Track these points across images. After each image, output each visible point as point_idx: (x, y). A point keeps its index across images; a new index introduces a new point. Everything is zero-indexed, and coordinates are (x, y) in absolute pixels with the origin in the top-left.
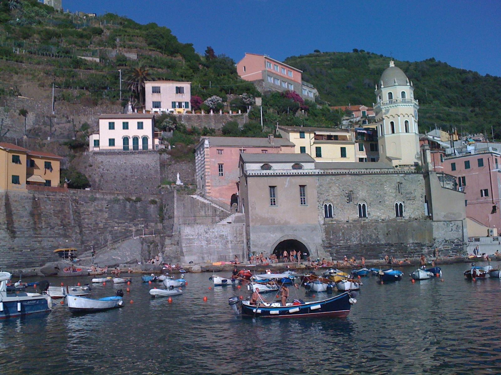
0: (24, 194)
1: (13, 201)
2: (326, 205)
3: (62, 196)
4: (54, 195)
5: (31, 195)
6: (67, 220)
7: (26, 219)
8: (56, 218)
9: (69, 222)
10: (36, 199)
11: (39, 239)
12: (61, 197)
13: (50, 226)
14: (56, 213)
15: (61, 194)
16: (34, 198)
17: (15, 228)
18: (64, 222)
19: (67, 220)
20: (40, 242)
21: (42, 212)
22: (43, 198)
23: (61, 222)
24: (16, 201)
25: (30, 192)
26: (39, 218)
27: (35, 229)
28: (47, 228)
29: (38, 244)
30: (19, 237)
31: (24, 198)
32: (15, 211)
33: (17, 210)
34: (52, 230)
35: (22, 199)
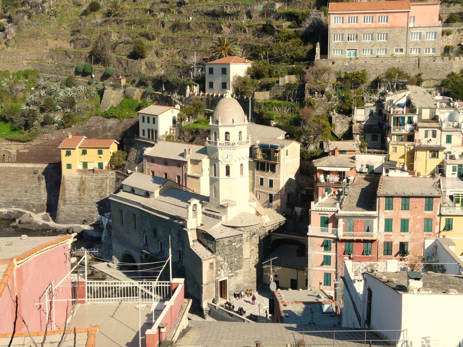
2: (146, 235)
3: (103, 176)
4: (96, 176)
5: (80, 176)
6: (104, 193)
7: (74, 192)
9: (105, 195)
11: (82, 206)
12: (101, 177)
14: (96, 188)
15: (102, 174)
16: (82, 178)
18: (102, 195)
19: (104, 193)
20: (82, 208)
21: (86, 188)
22: (88, 178)
23: (99, 194)
24: (69, 180)
27: (80, 199)
28: (88, 198)
29: (81, 209)
30: (68, 204)
32: (67, 188)
33: (69, 186)
34: (92, 200)
35: (74, 179)
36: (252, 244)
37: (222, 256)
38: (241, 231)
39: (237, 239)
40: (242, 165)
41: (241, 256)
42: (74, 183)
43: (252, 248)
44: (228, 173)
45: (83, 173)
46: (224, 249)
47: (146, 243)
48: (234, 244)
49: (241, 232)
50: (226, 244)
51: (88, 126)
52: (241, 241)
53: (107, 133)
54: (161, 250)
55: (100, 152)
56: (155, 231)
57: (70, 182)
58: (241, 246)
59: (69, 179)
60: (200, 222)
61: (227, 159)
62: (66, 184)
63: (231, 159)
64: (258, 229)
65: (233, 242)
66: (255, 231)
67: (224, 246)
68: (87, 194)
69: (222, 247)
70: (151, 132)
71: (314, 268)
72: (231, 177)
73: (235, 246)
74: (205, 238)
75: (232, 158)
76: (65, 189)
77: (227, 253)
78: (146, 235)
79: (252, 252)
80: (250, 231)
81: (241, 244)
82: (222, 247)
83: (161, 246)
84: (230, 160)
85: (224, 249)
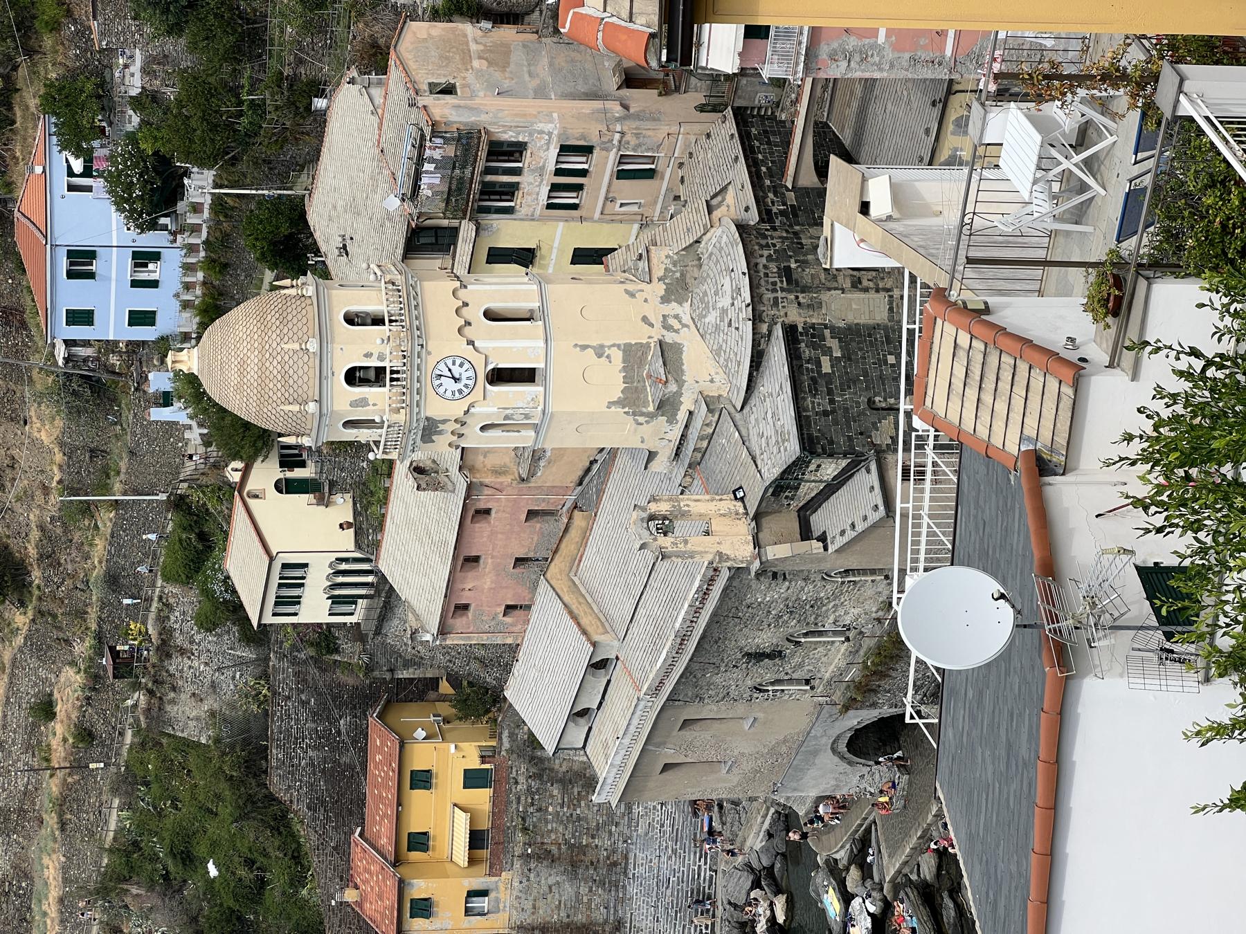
0: (516, 884)
1: (533, 913)
4: (519, 799)
7: (584, 890)
8: (583, 804)
10: (529, 851)
13: (605, 823)
14: (571, 800)
16: (526, 857)
17: (606, 921)
24: (534, 907)
25: (508, 866)
26: (583, 849)
28: (610, 832)
31: (525, 883)
34: (617, 819)
35: (527, 890)
36: (828, 285)
37: (874, 424)
38: (770, 332)
39: (807, 353)
40: (491, 315)
41: (880, 335)
42: (546, 889)
43: (847, 284)
44: (526, 376)
45: (505, 851)
46: (846, 410)
47: (807, 682)
48: (826, 368)
49: (778, 332)
50: (822, 402)
51: (309, 808)
52: (815, 333)
53: (339, 733)
54: (835, 633)
55: (423, 780)
56: (758, 656)
57: (540, 903)
58: (836, 332)
59: (528, 905)
60: (729, 504)
61: (464, 381)
62: (548, 919)
63: (461, 365)
64: (766, 253)
65: (819, 372)
66: (773, 267)
67: (833, 411)
68: (593, 837)
69: (836, 422)
70: (341, 579)
71: (949, 52)
72: (542, 365)
73: (835, 362)
74: (797, 488)
75: (458, 362)
76: (568, 925)
77: (863, 399)
78: (772, 684)
79: (865, 283)
80: (775, 291)
81: (827, 332)
82: (836, 422)
83: (820, 634)
84: (467, 365)
85: (846, 410)
